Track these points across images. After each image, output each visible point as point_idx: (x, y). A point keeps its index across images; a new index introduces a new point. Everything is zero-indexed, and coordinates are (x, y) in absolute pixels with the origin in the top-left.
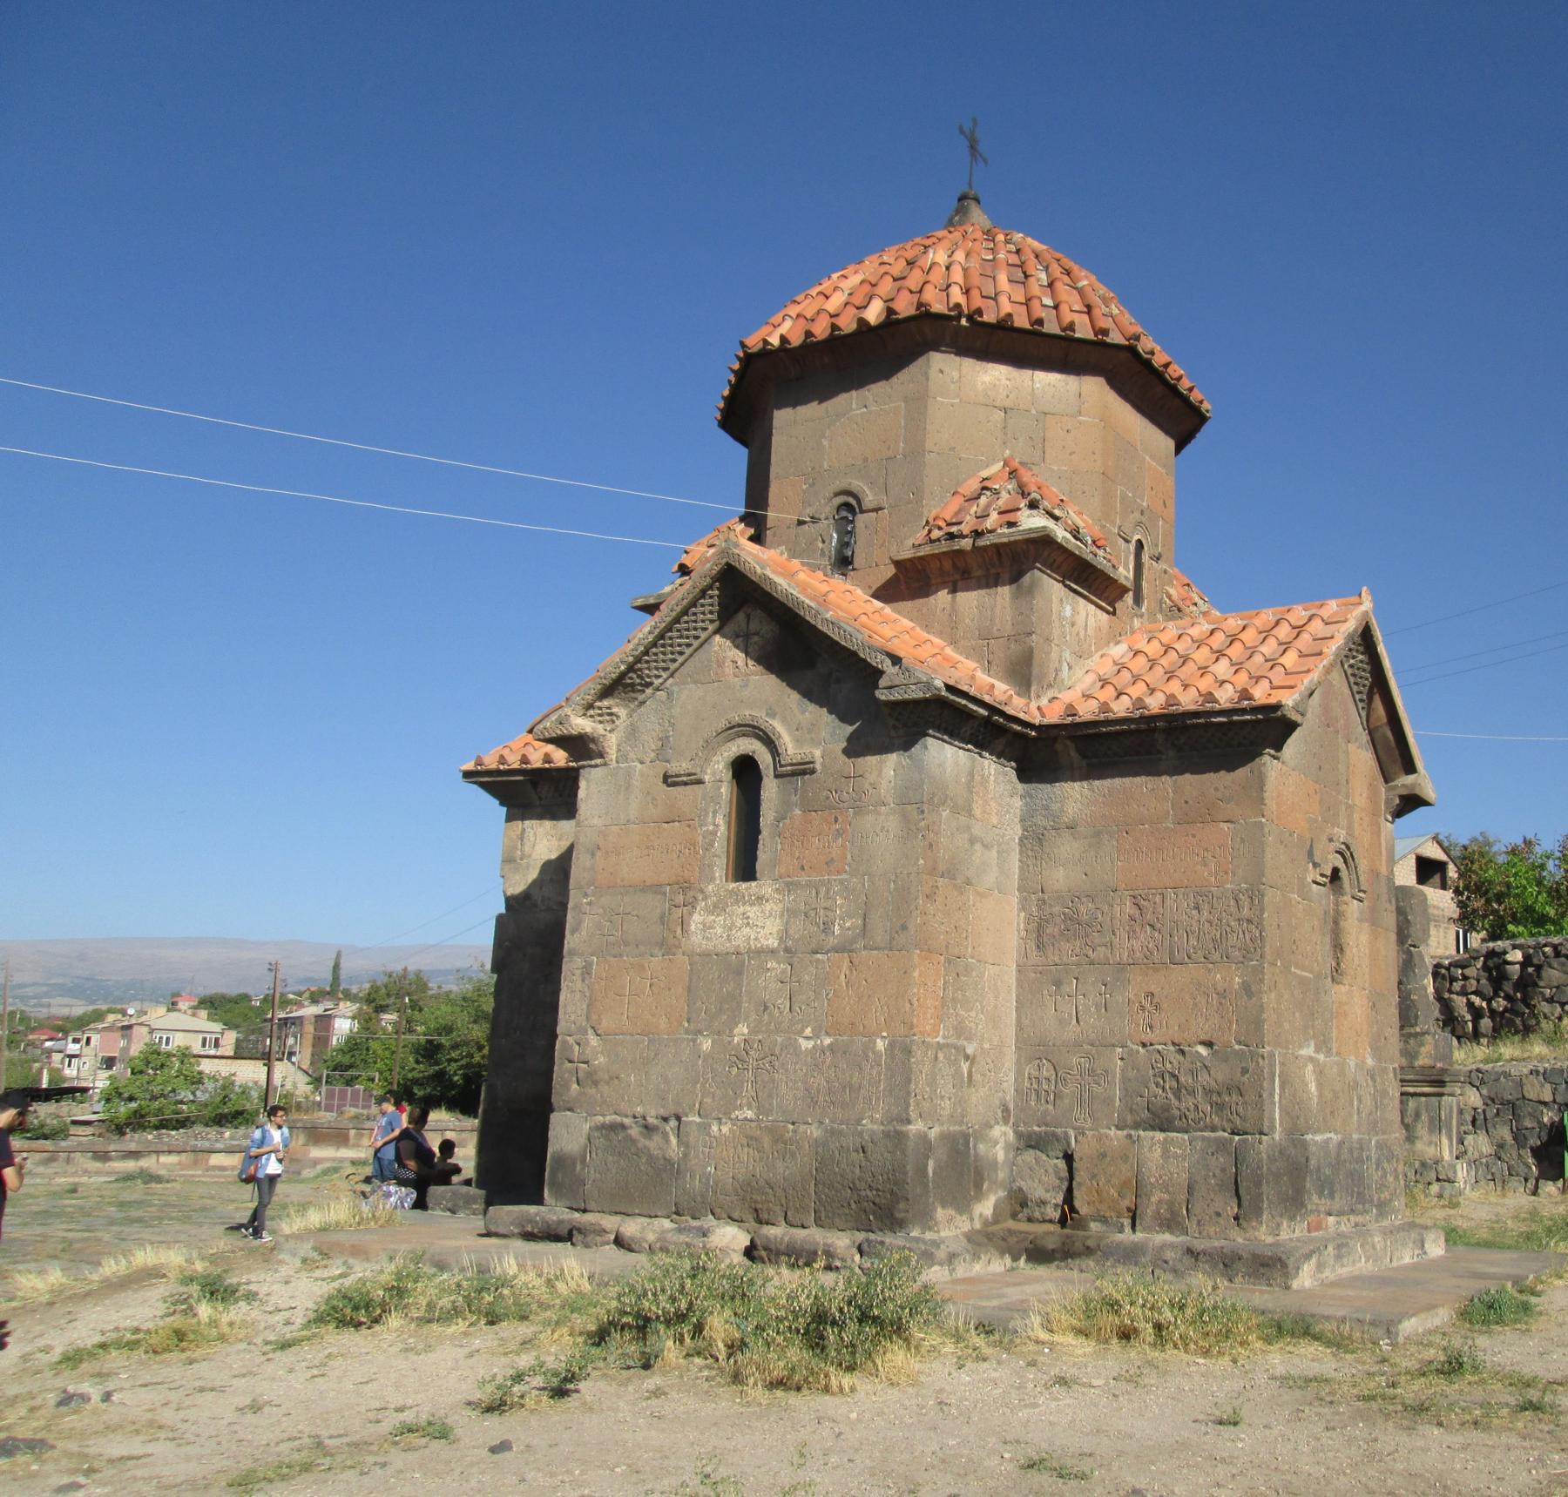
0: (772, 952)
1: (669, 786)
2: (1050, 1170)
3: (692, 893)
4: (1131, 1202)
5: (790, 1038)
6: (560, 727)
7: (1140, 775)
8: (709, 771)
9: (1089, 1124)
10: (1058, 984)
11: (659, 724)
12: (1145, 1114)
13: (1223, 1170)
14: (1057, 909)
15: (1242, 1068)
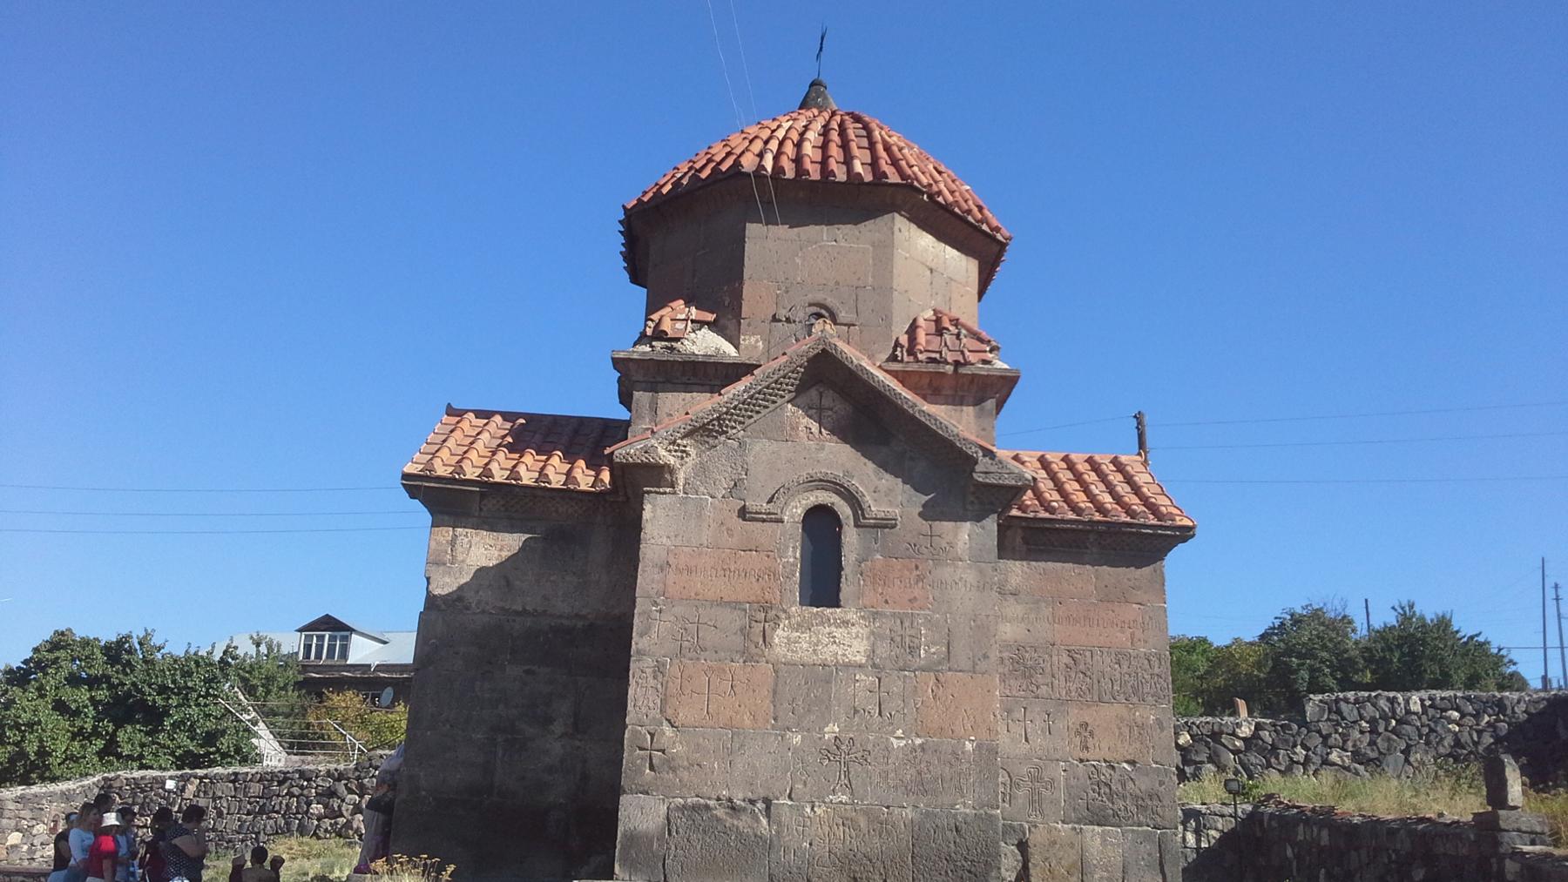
0: (860, 666)
1: (744, 520)
2: (1009, 854)
3: (774, 612)
4: (1078, 878)
5: (882, 737)
6: (646, 455)
7: (1068, 562)
8: (787, 513)
9: (1040, 819)
10: (1009, 712)
11: (731, 467)
12: (1086, 813)
13: (1149, 855)
14: (1005, 655)
15: (1160, 781)
